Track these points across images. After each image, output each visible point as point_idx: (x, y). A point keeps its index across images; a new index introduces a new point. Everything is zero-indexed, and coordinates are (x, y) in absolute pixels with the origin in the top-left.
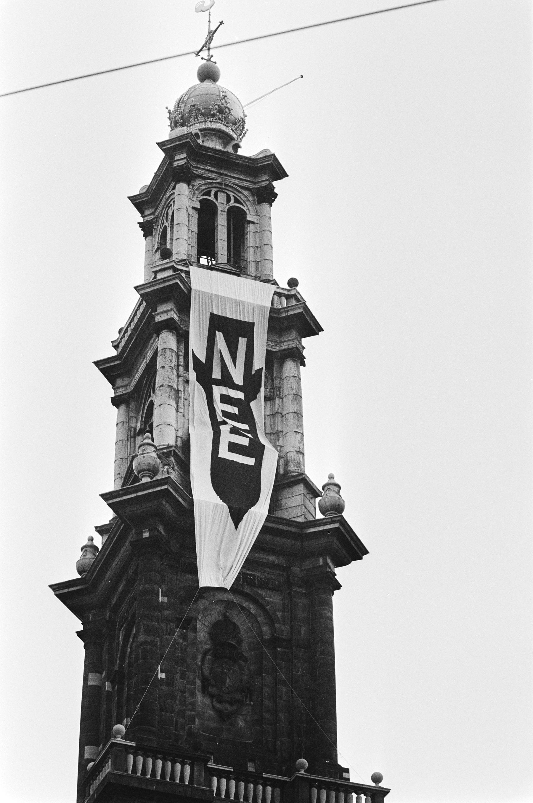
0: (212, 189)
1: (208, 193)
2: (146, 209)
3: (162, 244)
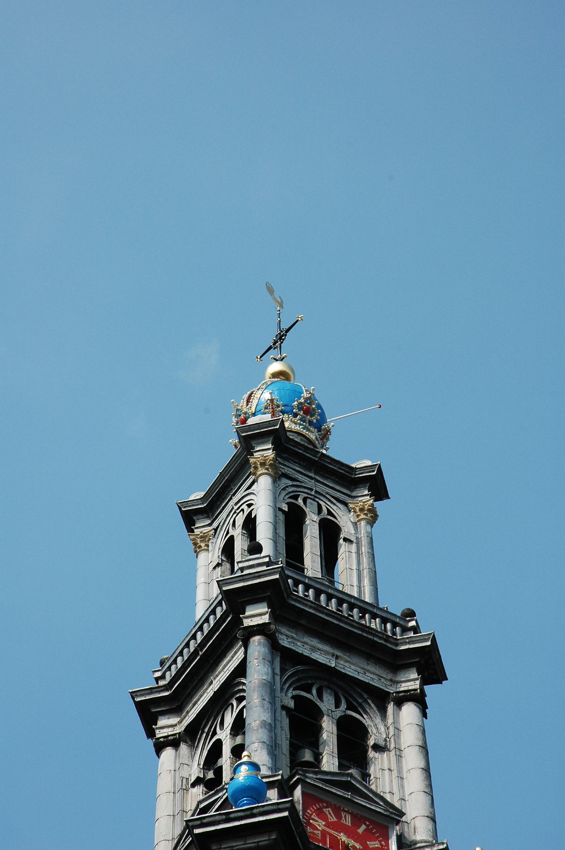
0: (300, 493)
1: (296, 497)
2: (198, 519)
3: (224, 561)
